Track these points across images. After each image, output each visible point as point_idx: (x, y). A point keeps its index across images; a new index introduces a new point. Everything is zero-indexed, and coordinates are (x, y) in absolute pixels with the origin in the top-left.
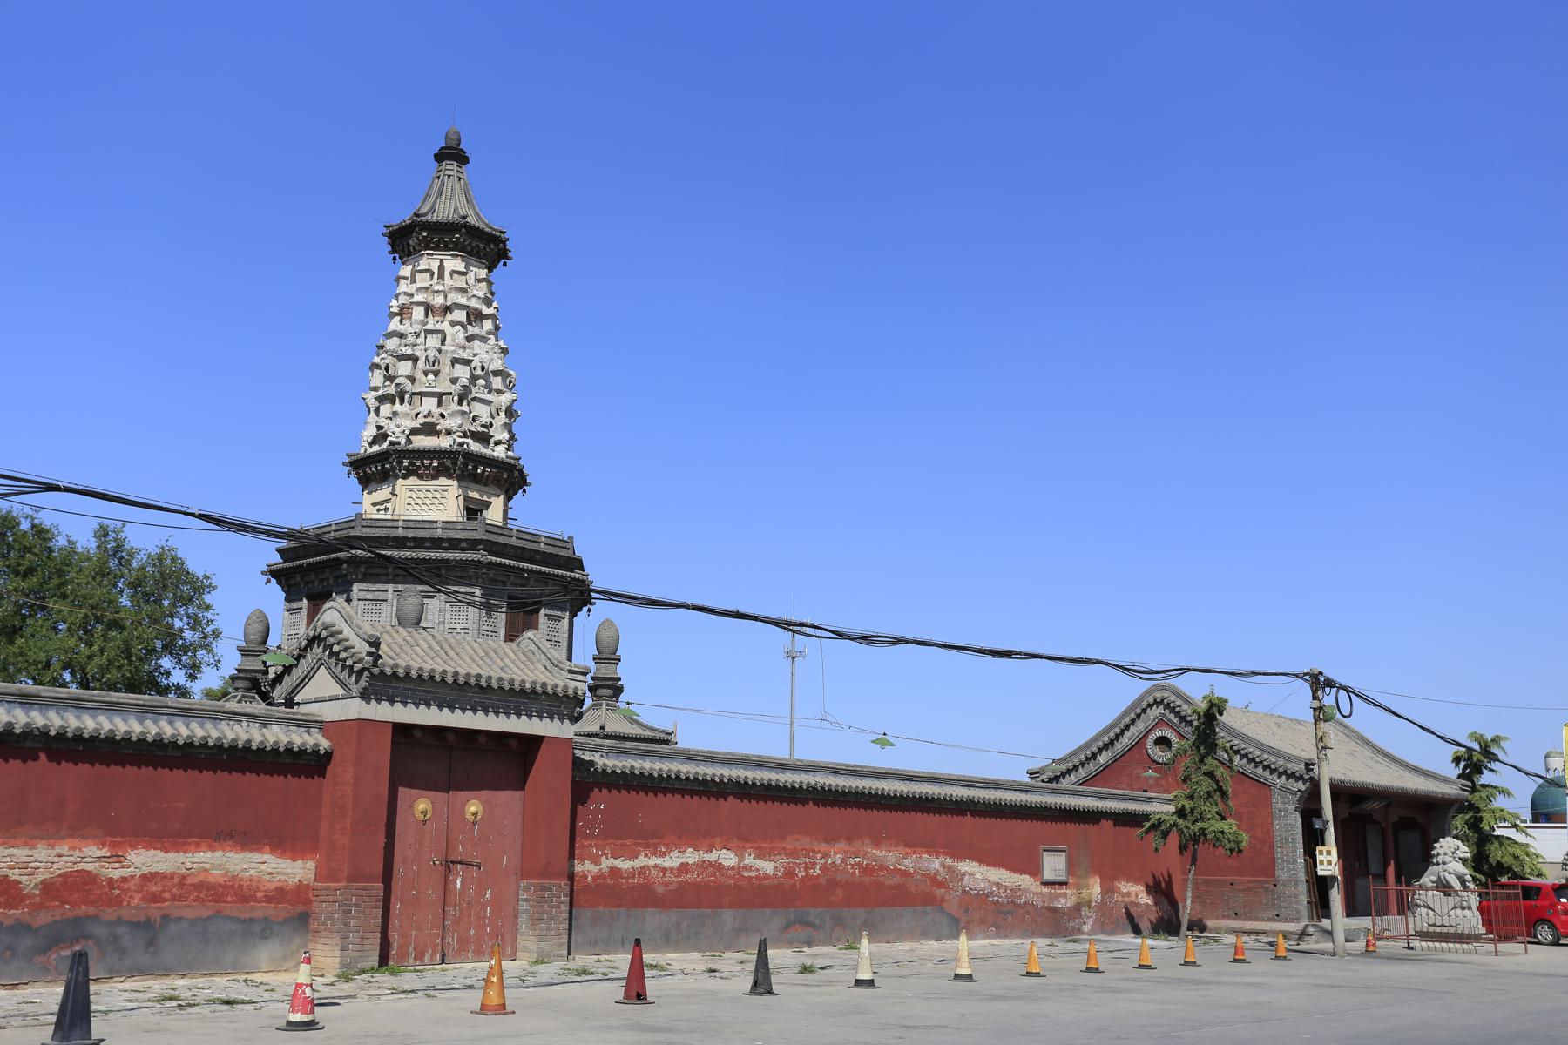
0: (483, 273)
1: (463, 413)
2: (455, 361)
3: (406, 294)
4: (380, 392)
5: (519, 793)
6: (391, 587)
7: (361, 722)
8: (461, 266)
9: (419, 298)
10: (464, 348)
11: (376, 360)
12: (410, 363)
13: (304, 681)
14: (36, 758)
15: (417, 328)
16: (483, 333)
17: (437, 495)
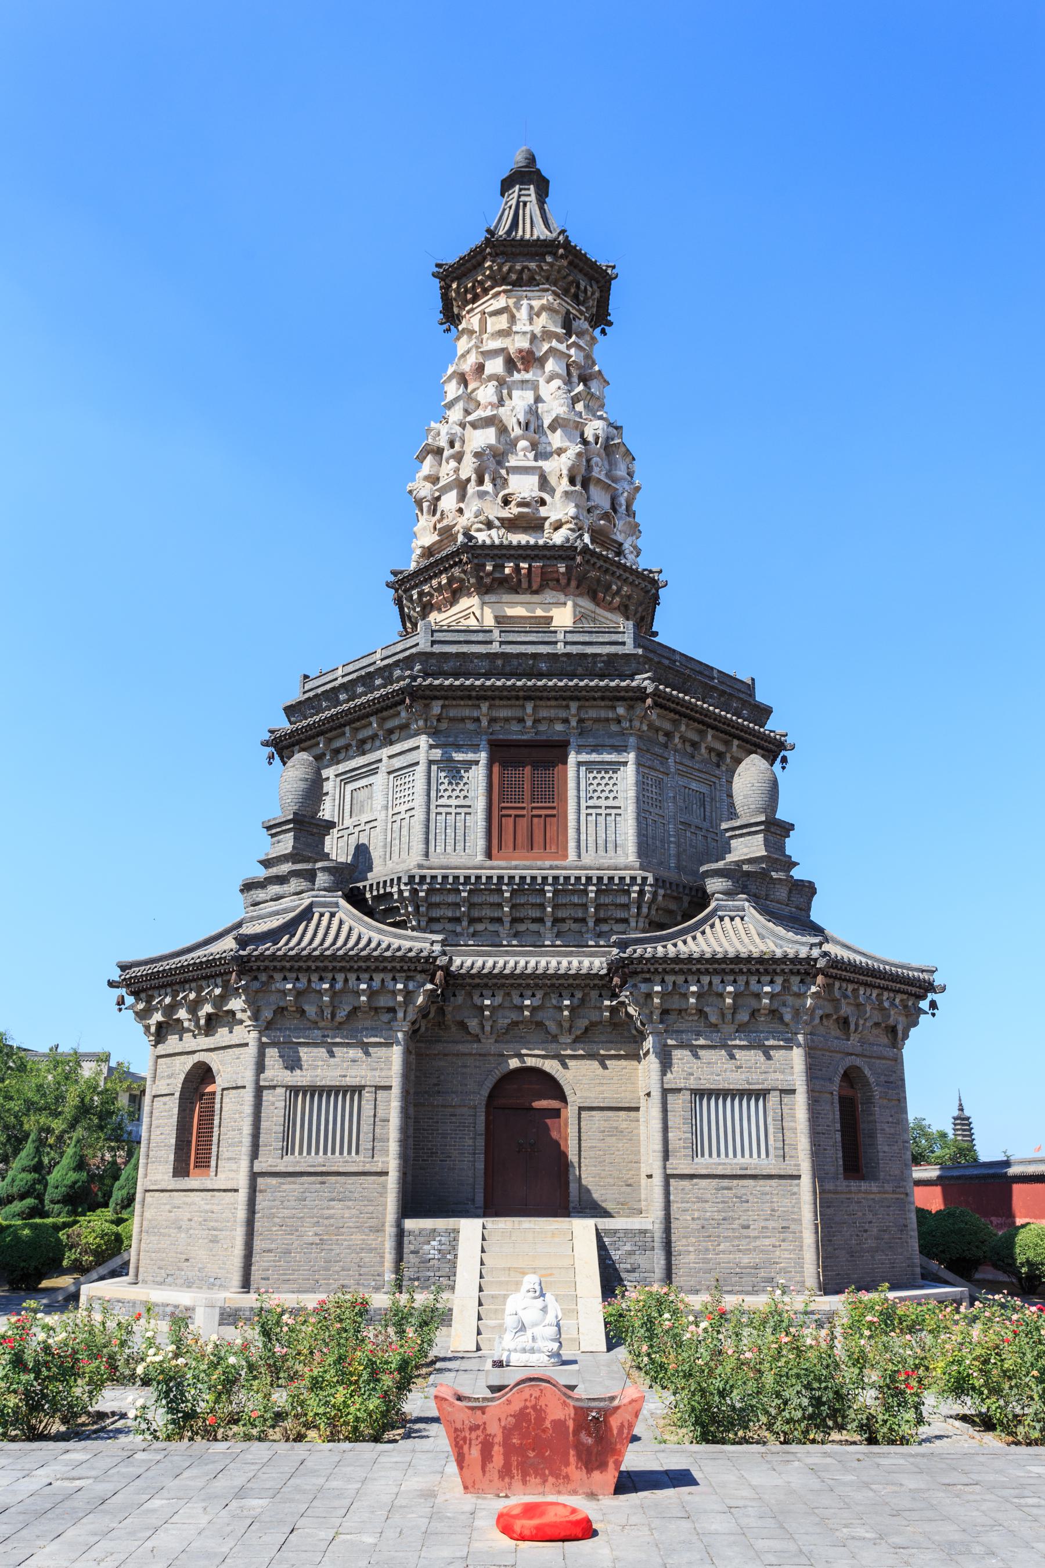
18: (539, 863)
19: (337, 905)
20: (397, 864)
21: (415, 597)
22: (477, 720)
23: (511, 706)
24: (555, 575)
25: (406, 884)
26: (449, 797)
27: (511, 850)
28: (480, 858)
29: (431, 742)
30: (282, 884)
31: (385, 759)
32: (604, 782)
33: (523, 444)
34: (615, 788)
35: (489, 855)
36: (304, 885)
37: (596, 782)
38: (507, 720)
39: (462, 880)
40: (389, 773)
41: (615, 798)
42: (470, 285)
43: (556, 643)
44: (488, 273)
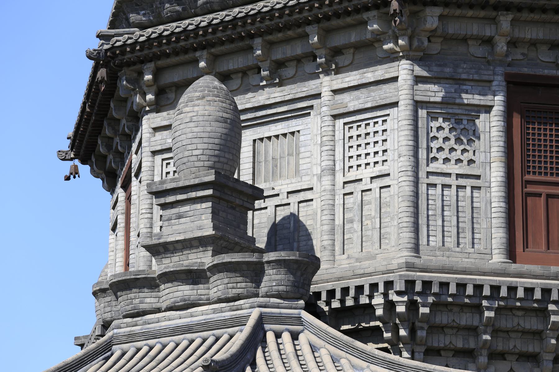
19: (299, 320)
20: (358, 260)
22: (489, 41)
23: (544, 23)
25: (399, 293)
26: (446, 160)
27: (544, 247)
28: (498, 258)
29: (419, 71)
30: (195, 283)
35: (511, 254)
36: (241, 285)
38: (534, 44)
39: (487, 291)
40: (335, 117)
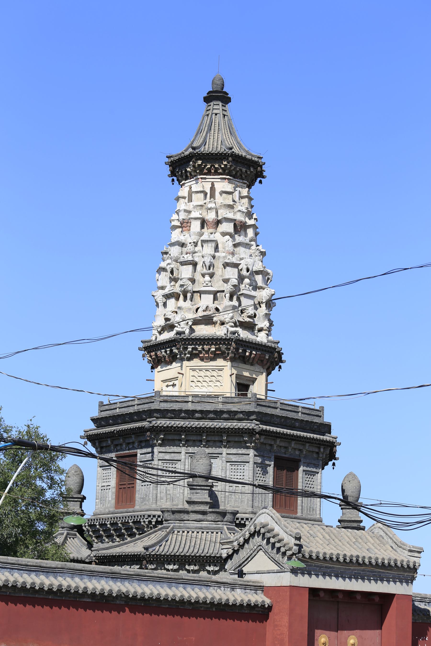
0: (245, 192)
1: (234, 308)
2: (226, 265)
3: (185, 211)
4: (167, 291)
5: (378, 631)
6: (183, 450)
7: (292, 588)
8: (229, 187)
9: (194, 214)
10: (233, 254)
11: (163, 264)
12: (190, 267)
13: (248, 560)
14: (124, 611)
15: (194, 238)
16: (247, 240)
17: (214, 373)
18: (291, 515)
21: (190, 349)
22: (271, 445)
24: (262, 359)
31: (224, 454)
32: (310, 480)
33: (247, 281)
34: (313, 483)
36: (220, 518)
37: (307, 479)
40: (227, 462)
41: (313, 488)
42: (209, 166)
43: (298, 412)
44: (223, 166)
